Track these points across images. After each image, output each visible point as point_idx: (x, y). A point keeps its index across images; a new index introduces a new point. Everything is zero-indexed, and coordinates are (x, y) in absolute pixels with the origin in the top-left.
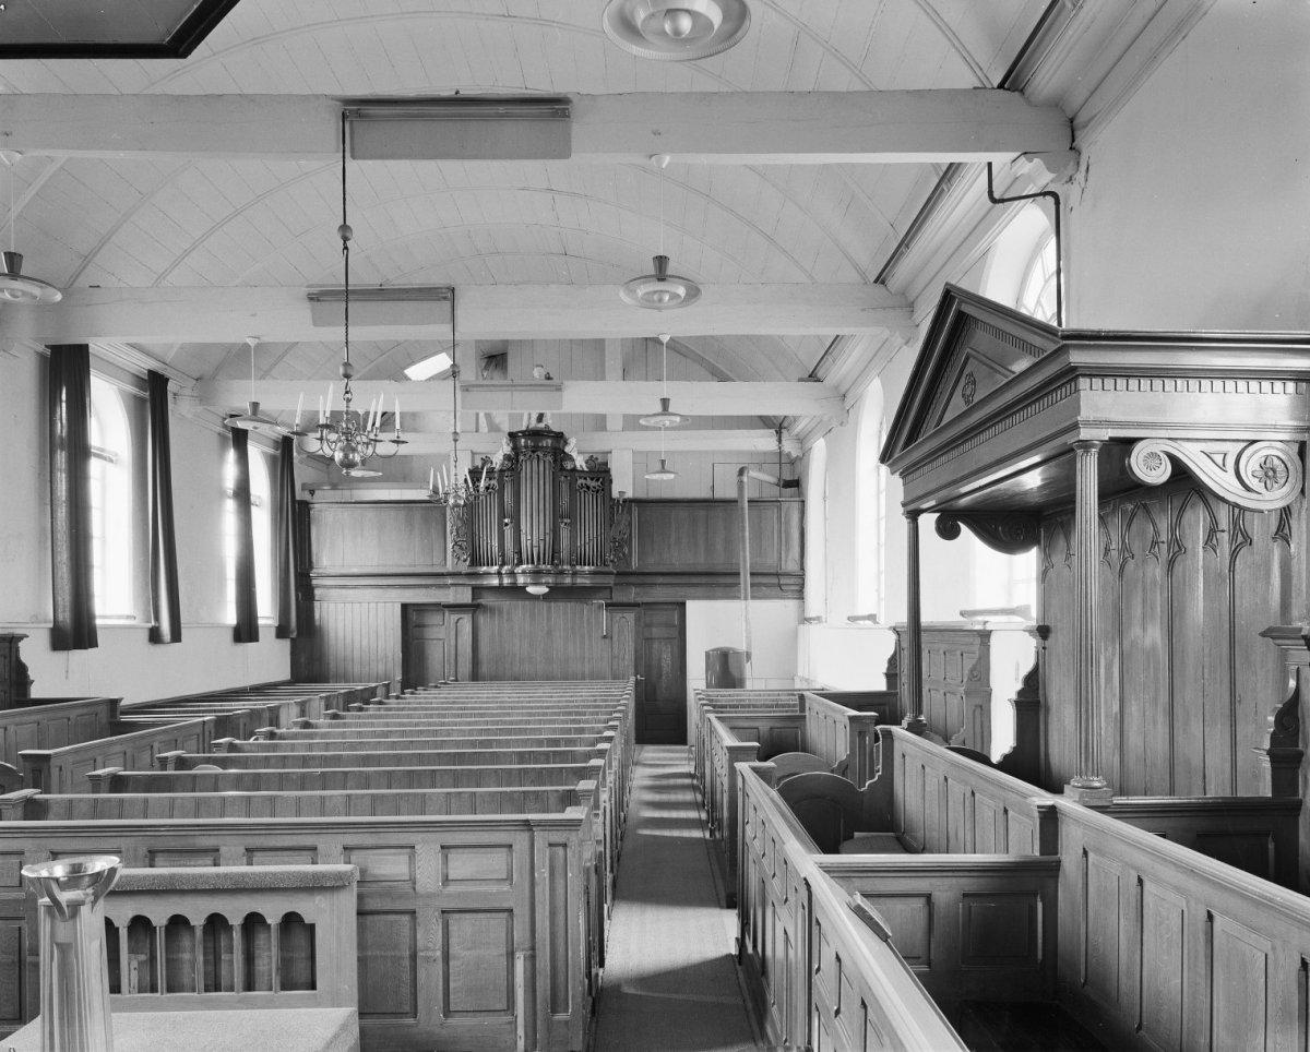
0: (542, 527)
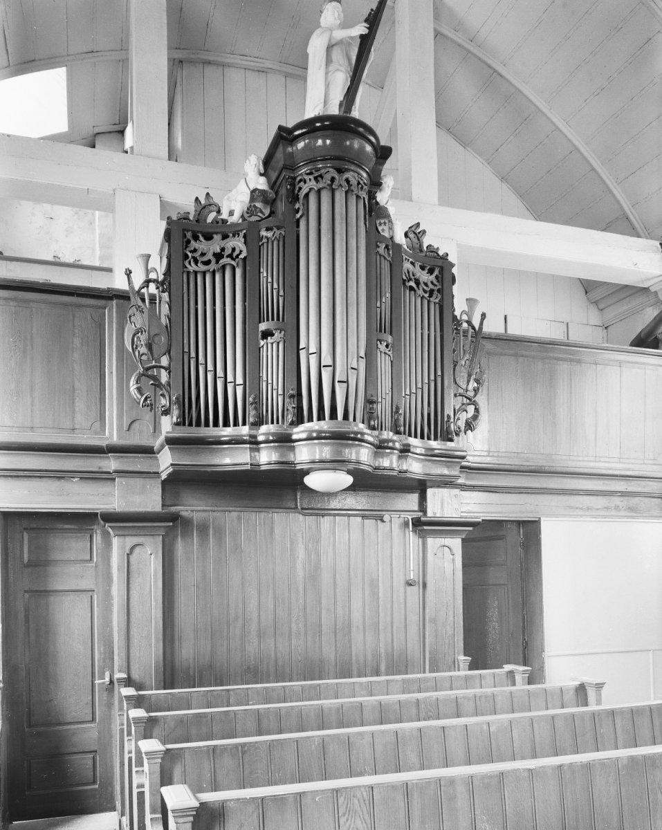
0: (353, 340)
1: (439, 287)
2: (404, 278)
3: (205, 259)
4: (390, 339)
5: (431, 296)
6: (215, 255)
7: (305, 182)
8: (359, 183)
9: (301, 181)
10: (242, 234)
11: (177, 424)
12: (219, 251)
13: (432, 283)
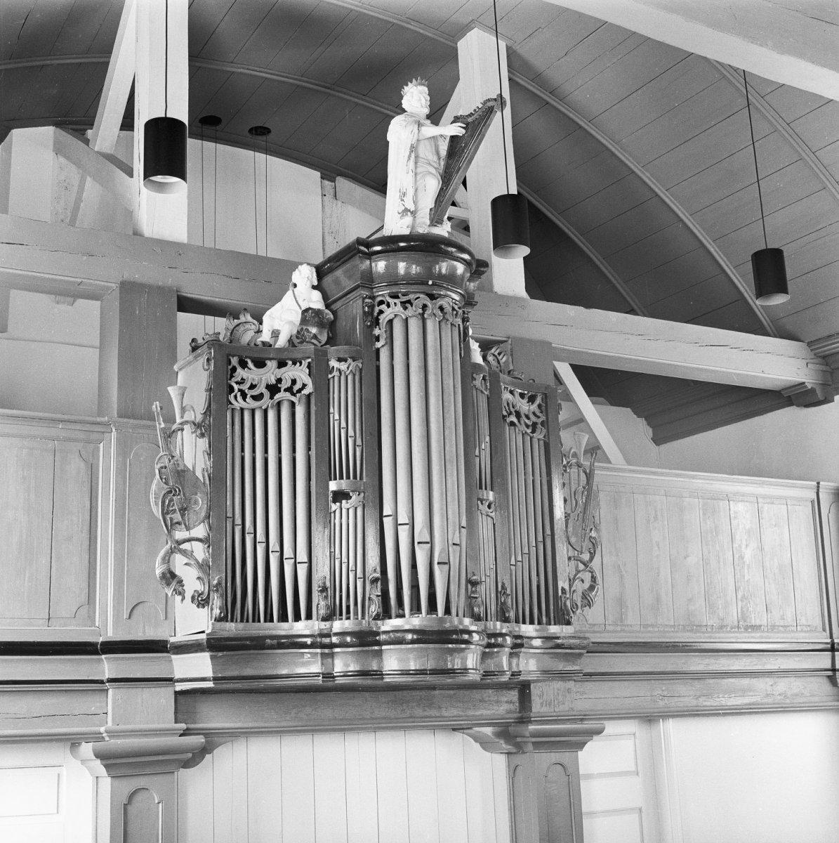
1: (543, 418)
2: (505, 413)
3: (255, 392)
4: (491, 496)
5: (533, 432)
6: (268, 387)
7: (388, 306)
8: (453, 309)
9: (381, 303)
10: (305, 363)
11: (219, 620)
12: (274, 382)
13: (534, 413)
